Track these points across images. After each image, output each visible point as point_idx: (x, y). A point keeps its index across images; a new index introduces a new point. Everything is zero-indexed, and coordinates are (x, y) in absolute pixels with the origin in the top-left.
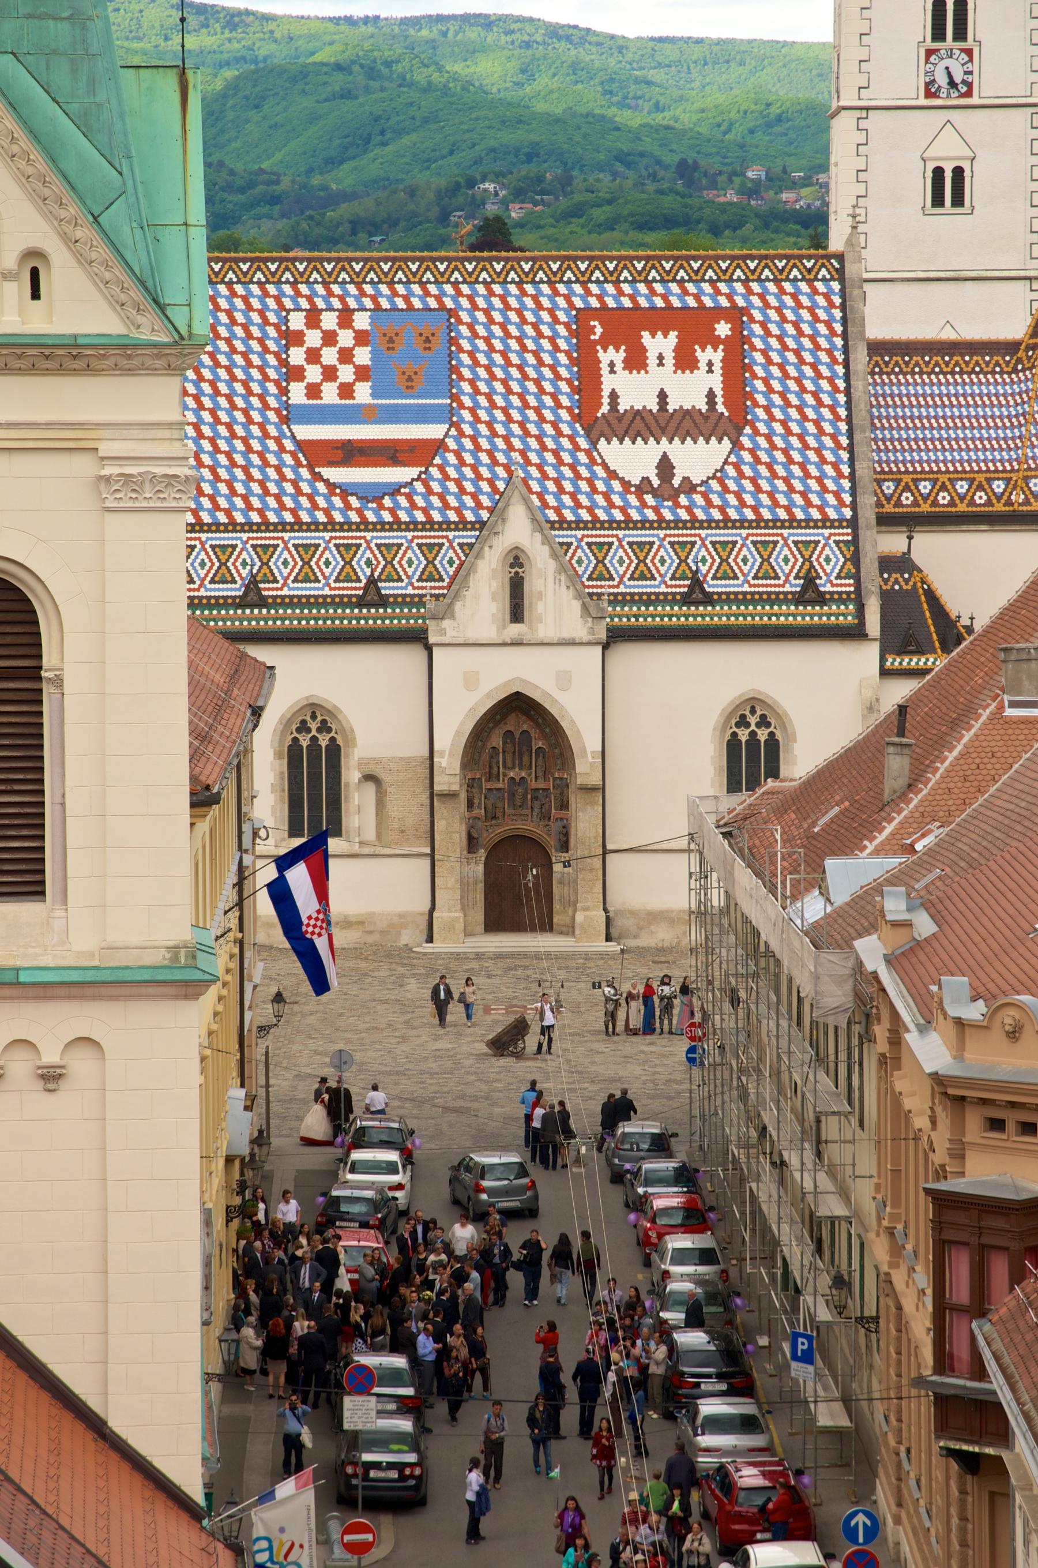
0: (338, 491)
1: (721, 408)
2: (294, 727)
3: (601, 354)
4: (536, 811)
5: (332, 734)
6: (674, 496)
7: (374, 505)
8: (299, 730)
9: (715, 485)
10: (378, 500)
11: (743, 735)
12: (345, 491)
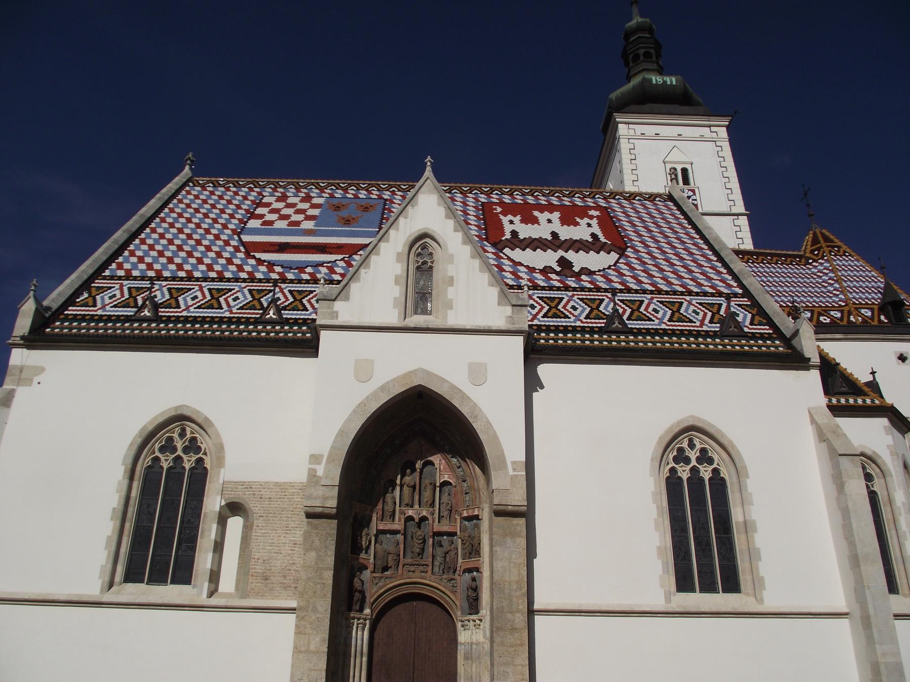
0: (266, 264)
1: (603, 239)
2: (157, 446)
3: (501, 217)
4: (439, 559)
5: (200, 455)
6: (577, 275)
7: (297, 271)
8: (162, 449)
9: (610, 271)
10: (301, 269)
11: (684, 473)
12: (271, 265)
